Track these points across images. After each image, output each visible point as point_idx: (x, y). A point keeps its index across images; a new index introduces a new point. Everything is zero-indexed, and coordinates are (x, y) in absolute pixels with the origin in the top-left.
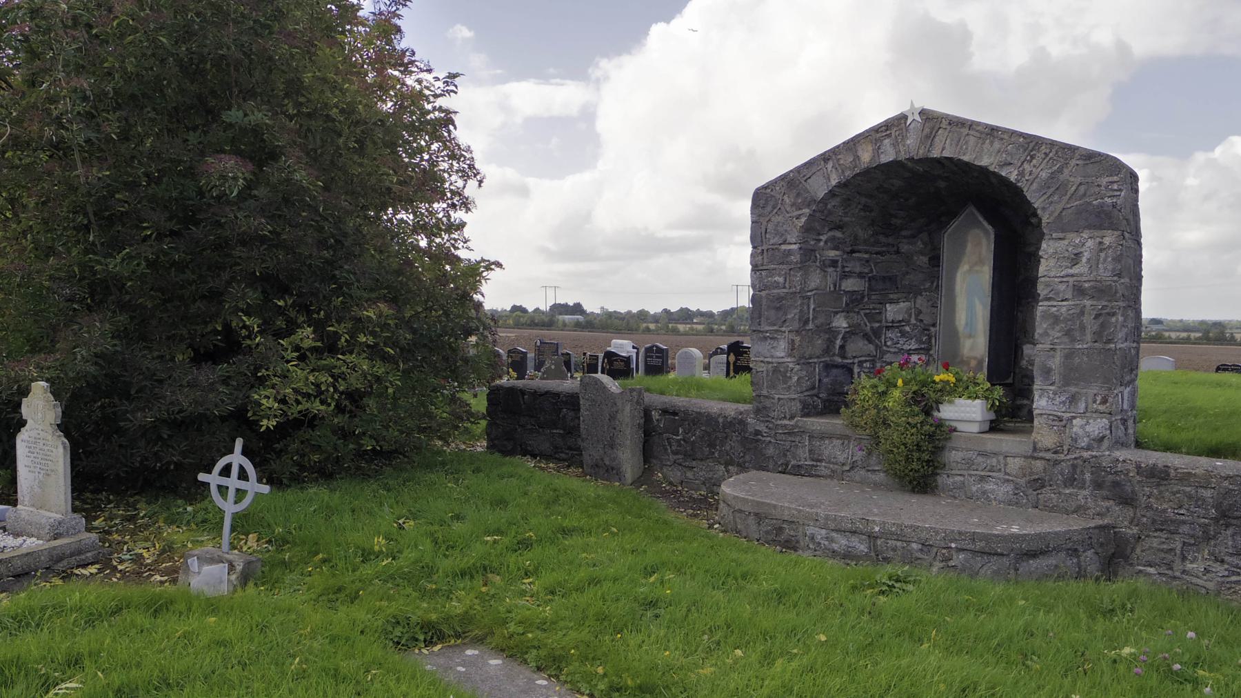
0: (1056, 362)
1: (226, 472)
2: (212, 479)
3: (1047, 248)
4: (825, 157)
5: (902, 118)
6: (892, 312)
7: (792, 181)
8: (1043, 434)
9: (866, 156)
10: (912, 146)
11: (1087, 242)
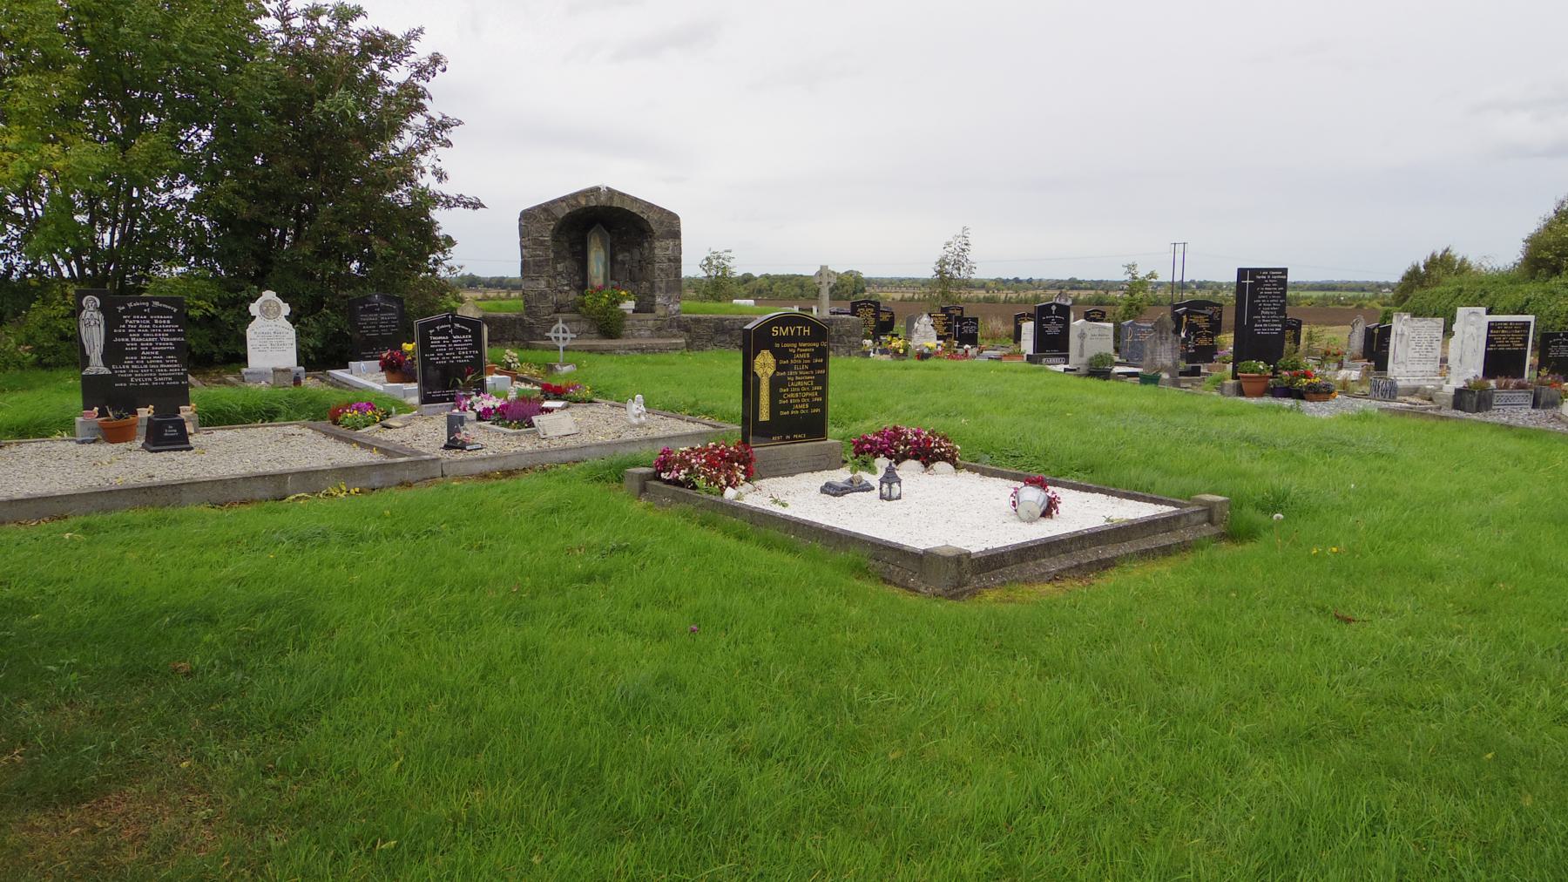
0: (663, 285)
1: (557, 331)
2: (552, 335)
3: (657, 244)
6: (560, 267)
7: (546, 208)
8: (660, 312)
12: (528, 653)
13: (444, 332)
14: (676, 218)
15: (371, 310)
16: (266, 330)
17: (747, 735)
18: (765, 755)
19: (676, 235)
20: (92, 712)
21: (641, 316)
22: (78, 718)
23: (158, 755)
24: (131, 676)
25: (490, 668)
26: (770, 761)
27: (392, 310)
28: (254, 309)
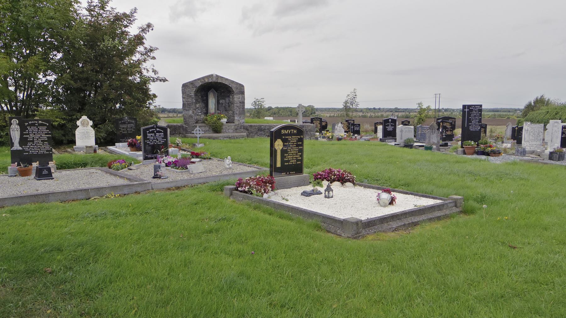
0: (238, 112)
2: (194, 132)
3: (235, 96)
4: (199, 79)
5: (212, 75)
6: (198, 106)
7: (192, 83)
9: (207, 81)
10: (214, 80)
11: (241, 96)
12: (187, 263)
13: (153, 132)
14: (243, 86)
15: (124, 123)
16: (83, 131)
17: (276, 297)
18: (282, 306)
19: (242, 93)
20: (12, 289)
21: (229, 124)
22: (7, 292)
23: (38, 307)
24: (28, 274)
25: (171, 269)
26: (285, 309)
27: (132, 123)
28: (78, 123)
